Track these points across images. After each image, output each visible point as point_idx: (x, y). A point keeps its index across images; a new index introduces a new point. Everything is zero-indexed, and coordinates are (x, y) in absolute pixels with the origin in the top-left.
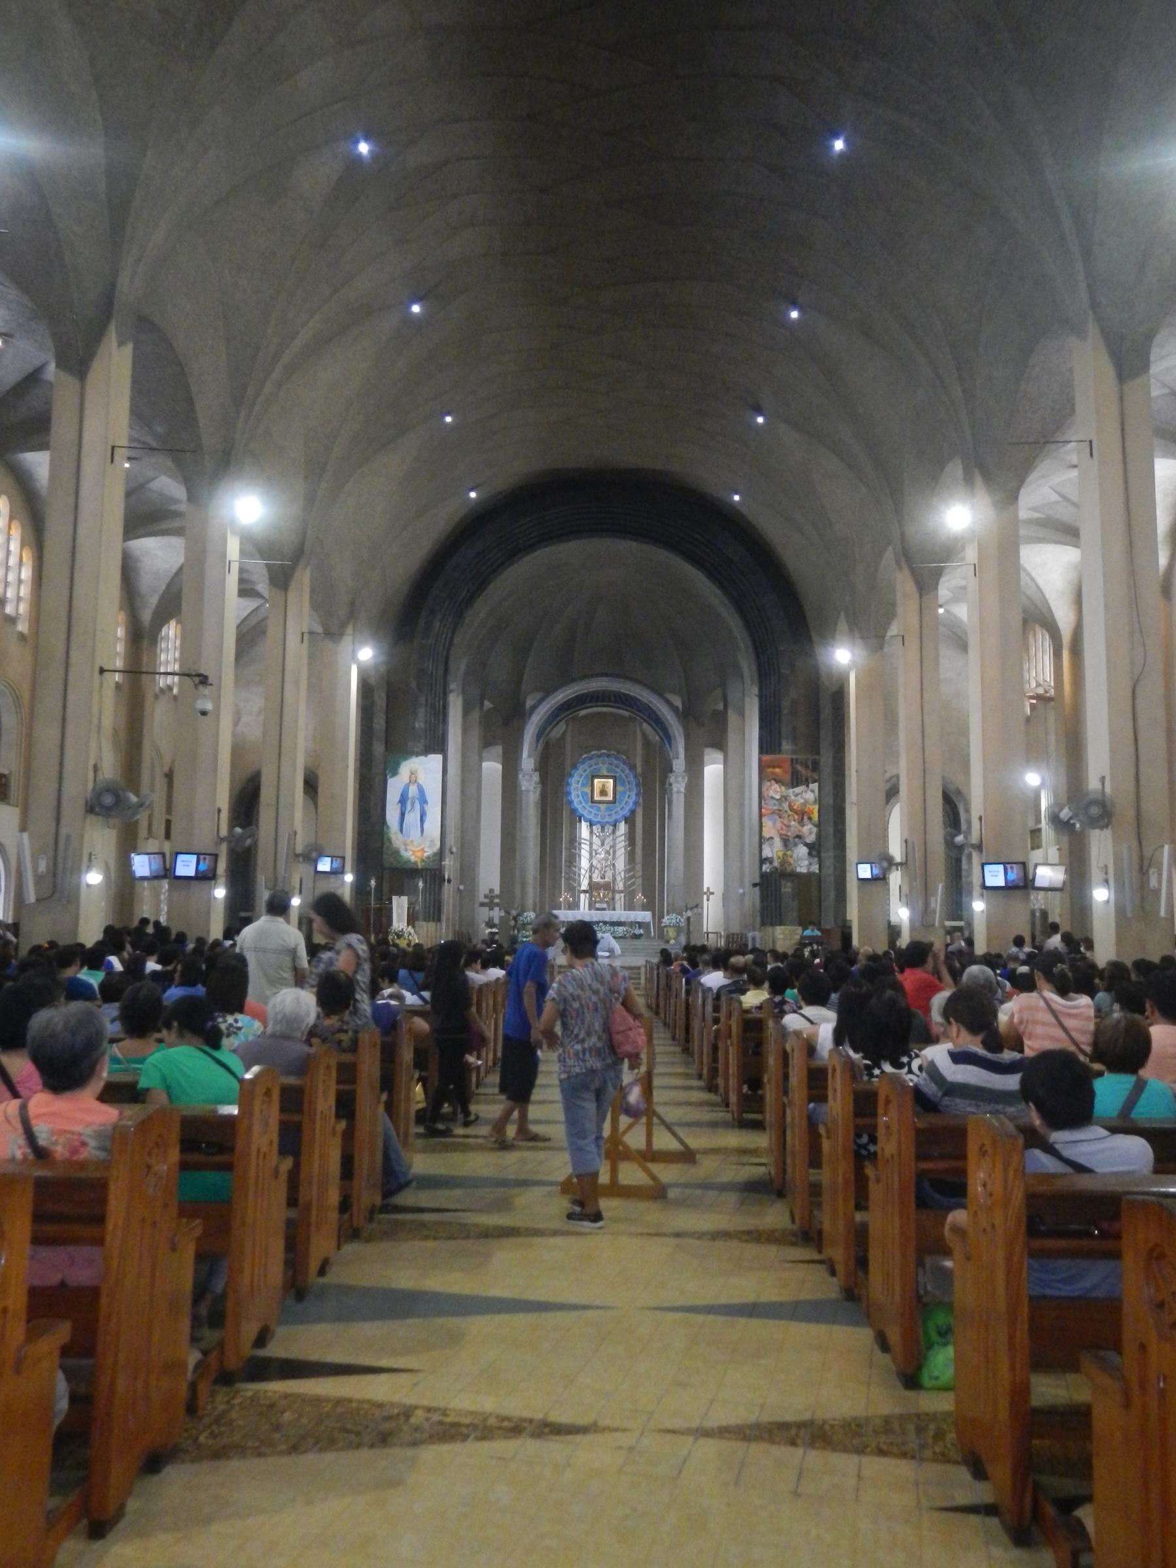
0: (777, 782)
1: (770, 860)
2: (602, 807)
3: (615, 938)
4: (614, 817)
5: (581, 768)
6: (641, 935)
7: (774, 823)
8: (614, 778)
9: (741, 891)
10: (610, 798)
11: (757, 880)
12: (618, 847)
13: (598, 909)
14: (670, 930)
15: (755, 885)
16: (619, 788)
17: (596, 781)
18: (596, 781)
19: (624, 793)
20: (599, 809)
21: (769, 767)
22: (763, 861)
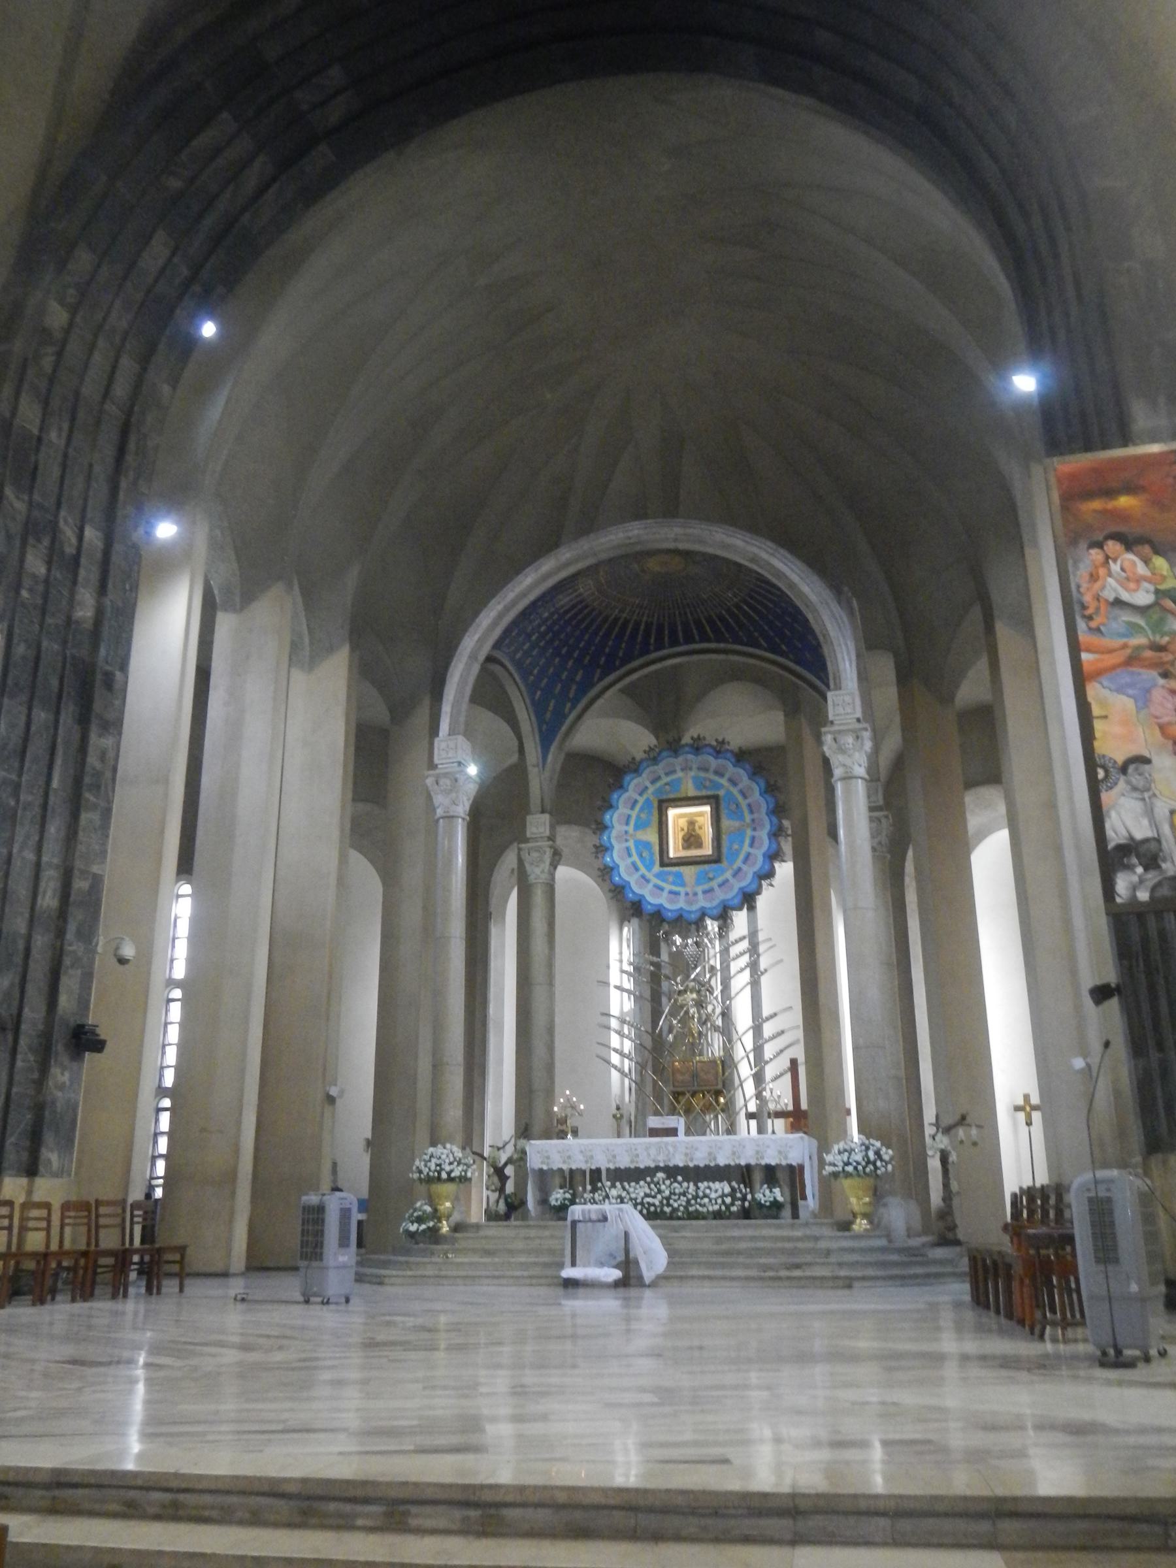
0: (1129, 543)
1: (1146, 853)
2: (688, 872)
3: (652, 1215)
4: (721, 896)
5: (633, 784)
6: (776, 1206)
7: (1143, 699)
8: (714, 801)
9: (1079, 1063)
10: (708, 850)
11: (1111, 977)
12: (734, 967)
13: (654, 1133)
14: (847, 1183)
15: (1101, 993)
16: (726, 823)
17: (672, 813)
18: (672, 813)
19: (740, 832)
20: (680, 880)
21: (1089, 495)
22: (1112, 858)
